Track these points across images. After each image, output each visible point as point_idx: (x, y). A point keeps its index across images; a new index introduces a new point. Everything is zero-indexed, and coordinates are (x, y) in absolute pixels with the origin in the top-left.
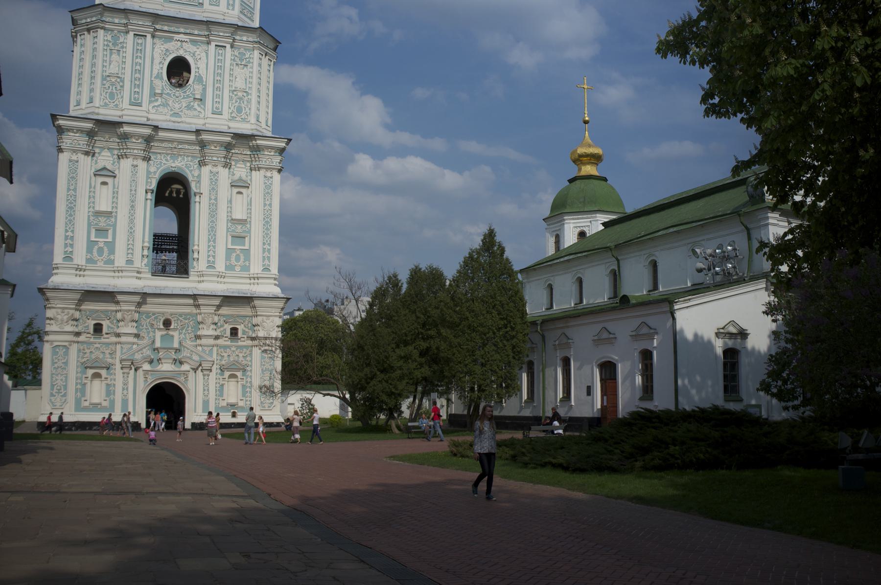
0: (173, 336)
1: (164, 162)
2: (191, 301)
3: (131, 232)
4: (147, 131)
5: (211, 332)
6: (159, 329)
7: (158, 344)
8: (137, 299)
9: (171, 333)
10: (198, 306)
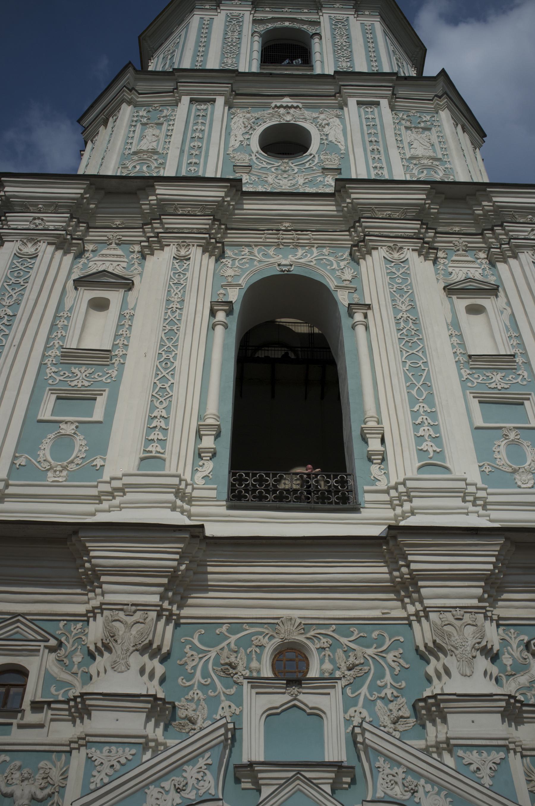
0: (317, 714)
1: (260, 256)
2: (377, 571)
3: (162, 390)
4: (215, 194)
5: (481, 686)
6: (257, 682)
7: (254, 747)
8: (165, 556)
9: (310, 700)
10: (406, 587)
